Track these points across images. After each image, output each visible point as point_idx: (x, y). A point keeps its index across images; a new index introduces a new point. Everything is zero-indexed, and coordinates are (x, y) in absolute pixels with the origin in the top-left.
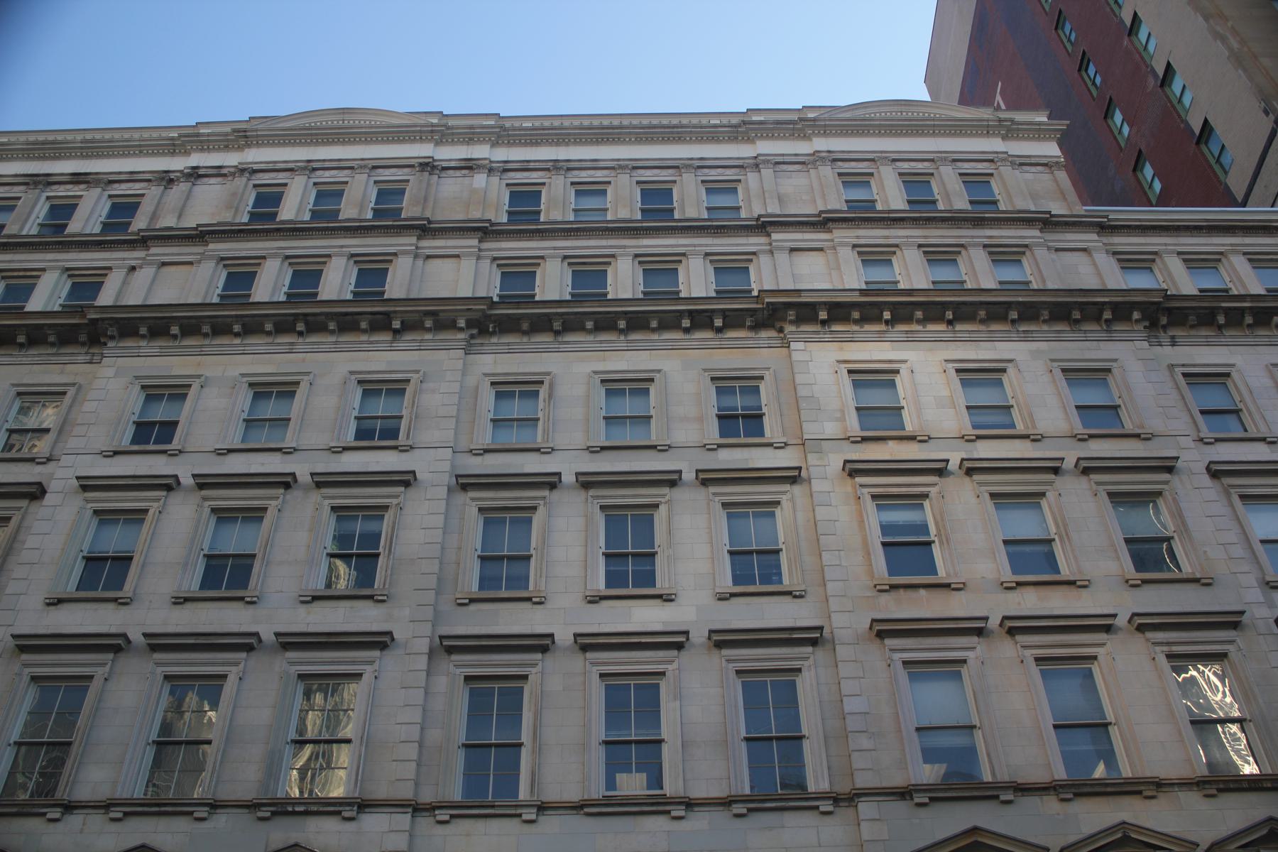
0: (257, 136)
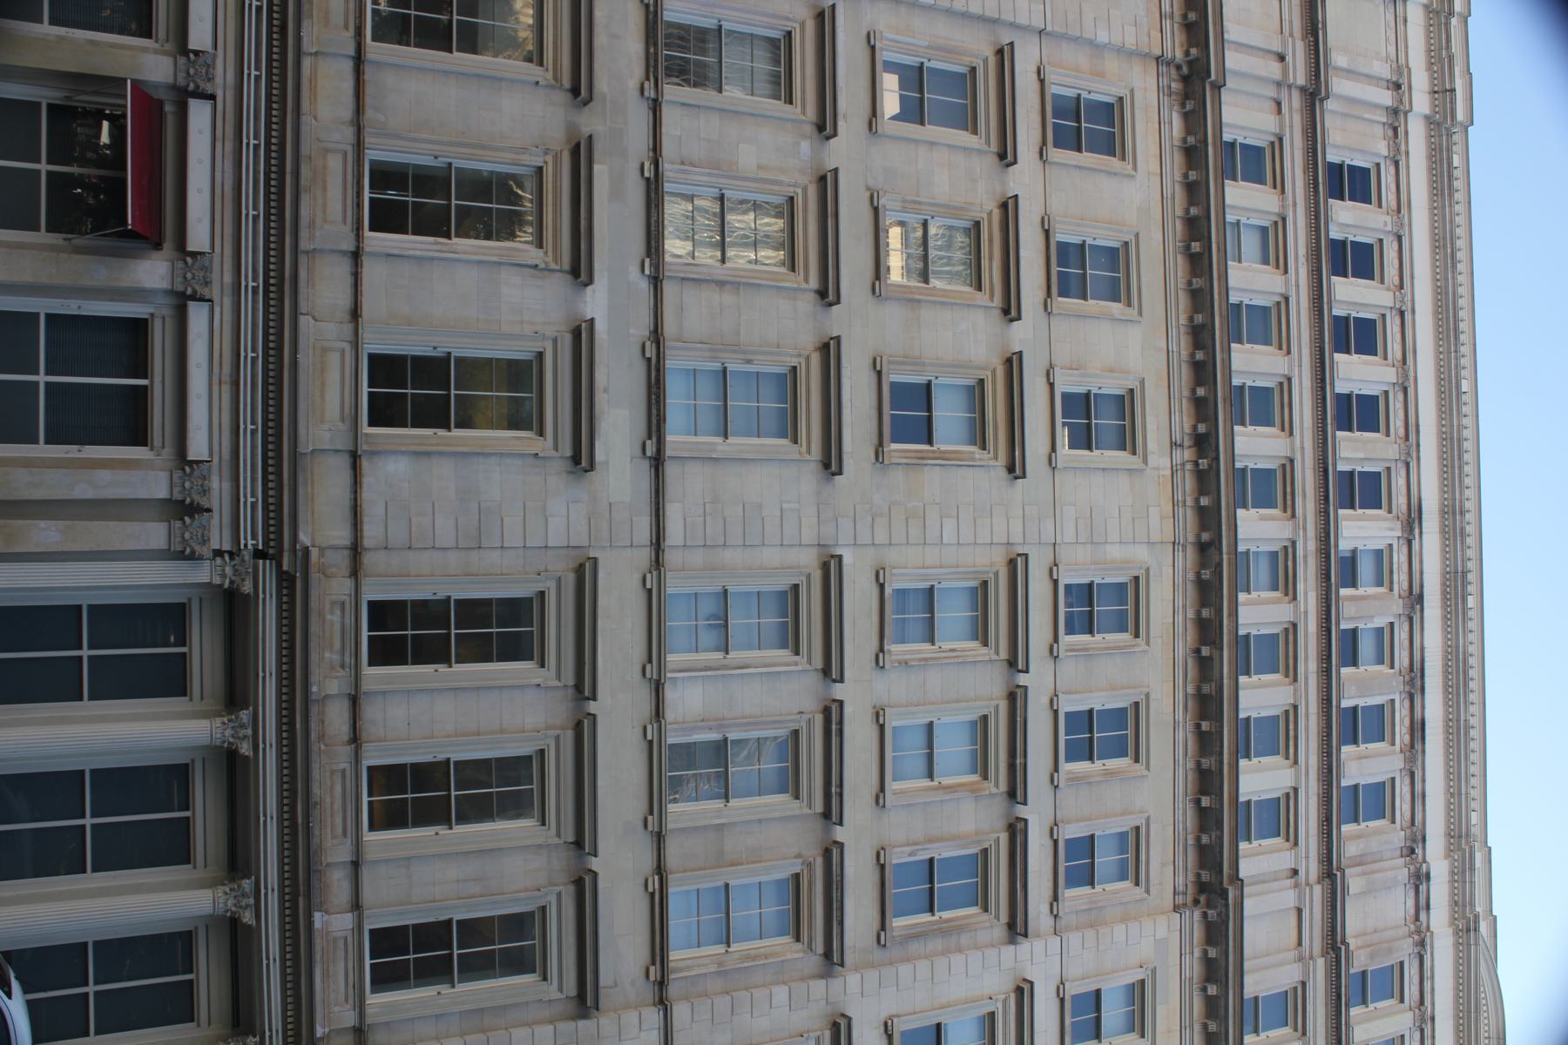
0: (1469, 945)
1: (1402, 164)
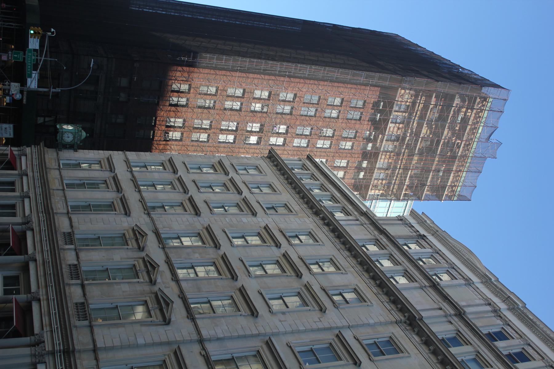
1: (510, 324)
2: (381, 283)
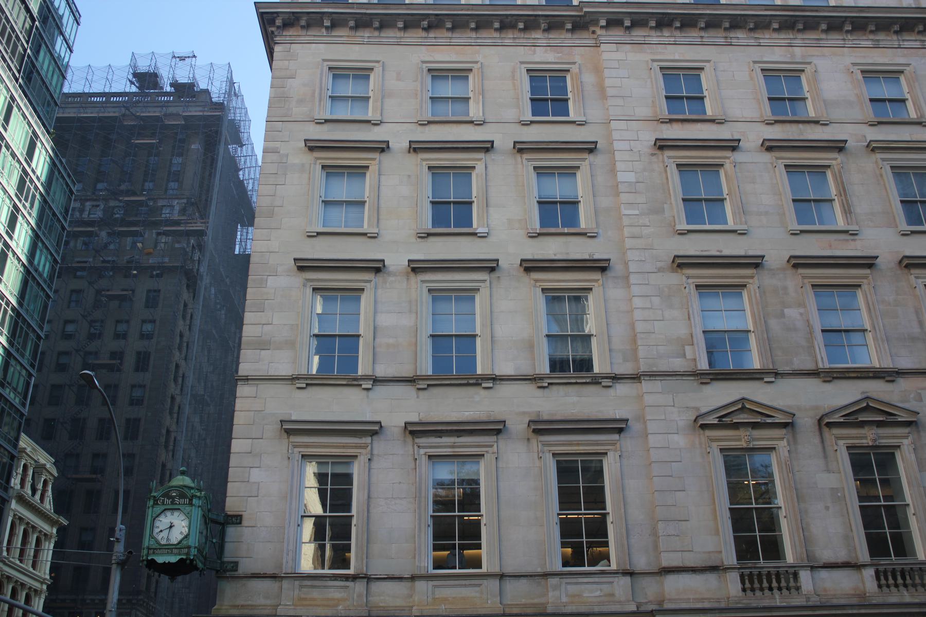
2: (852, 23)
